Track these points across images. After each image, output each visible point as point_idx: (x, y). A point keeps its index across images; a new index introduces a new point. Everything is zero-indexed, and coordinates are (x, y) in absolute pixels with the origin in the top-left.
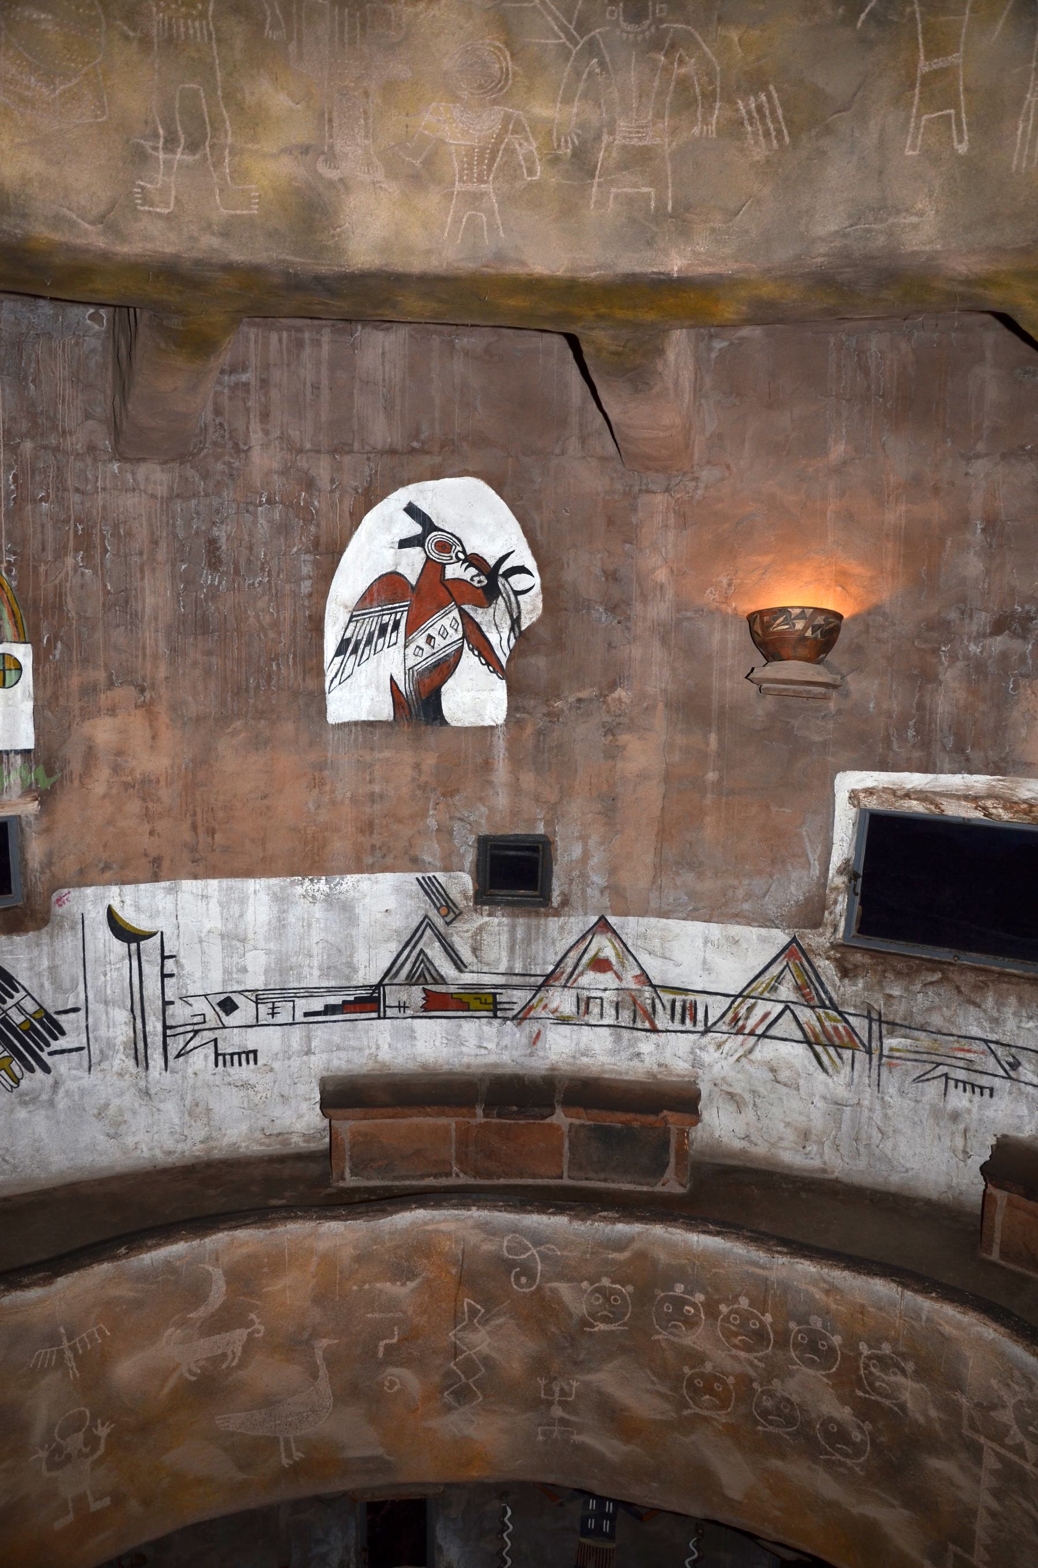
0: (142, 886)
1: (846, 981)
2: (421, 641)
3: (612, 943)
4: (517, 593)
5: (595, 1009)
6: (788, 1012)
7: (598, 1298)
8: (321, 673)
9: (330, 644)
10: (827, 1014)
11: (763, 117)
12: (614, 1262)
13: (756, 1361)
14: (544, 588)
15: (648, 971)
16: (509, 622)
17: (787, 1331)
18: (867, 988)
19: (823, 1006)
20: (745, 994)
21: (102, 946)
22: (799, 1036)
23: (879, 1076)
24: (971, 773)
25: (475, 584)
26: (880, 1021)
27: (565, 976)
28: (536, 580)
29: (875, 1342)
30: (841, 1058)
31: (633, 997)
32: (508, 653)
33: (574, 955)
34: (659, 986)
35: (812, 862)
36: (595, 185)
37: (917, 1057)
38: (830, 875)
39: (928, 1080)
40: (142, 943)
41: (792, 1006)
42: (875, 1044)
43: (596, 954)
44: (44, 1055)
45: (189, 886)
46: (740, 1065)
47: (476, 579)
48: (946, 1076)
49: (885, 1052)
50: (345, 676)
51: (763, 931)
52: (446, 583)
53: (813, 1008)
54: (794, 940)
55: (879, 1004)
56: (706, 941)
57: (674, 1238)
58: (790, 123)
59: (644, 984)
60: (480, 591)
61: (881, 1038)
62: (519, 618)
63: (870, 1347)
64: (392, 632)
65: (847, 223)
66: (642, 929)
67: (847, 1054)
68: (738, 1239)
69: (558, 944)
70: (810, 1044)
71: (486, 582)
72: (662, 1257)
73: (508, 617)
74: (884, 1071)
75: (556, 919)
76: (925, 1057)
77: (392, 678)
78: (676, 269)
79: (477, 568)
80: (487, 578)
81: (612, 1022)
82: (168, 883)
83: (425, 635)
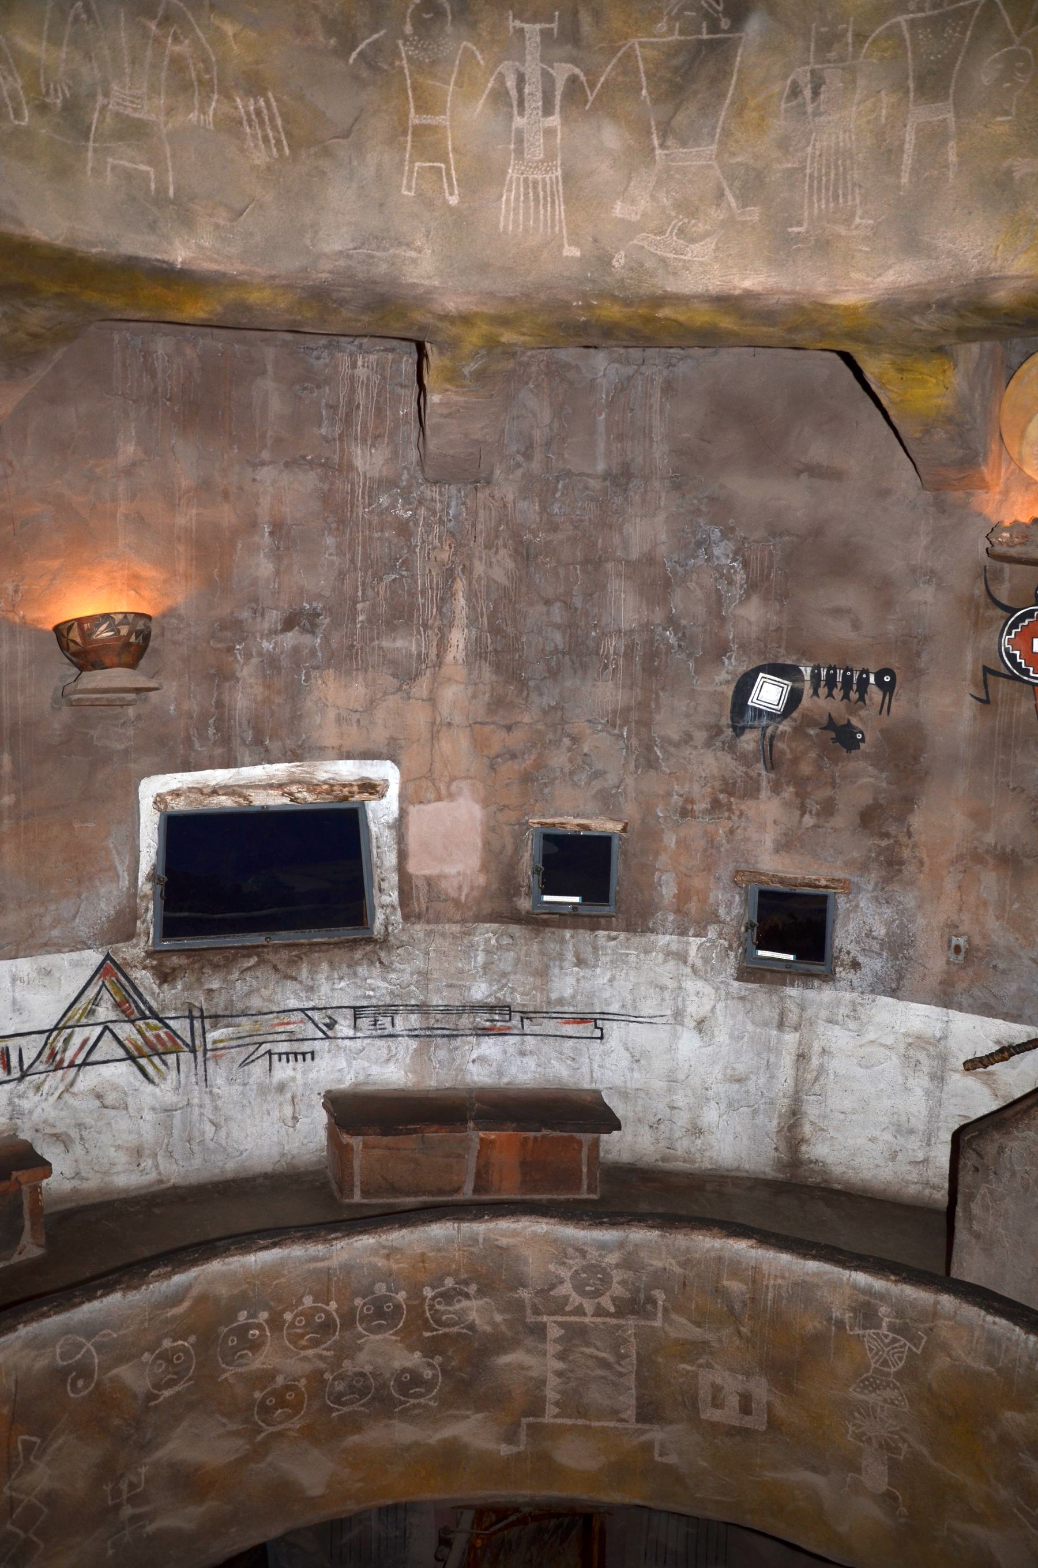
1: (165, 986)
6: (107, 1033)
7: (161, 1365)
10: (147, 1024)
11: (262, 123)
12: (174, 1318)
13: (325, 1353)
17: (353, 1309)
18: (187, 988)
19: (144, 1017)
20: (60, 1025)
22: (121, 1053)
23: (206, 1071)
24: (270, 762)
29: (437, 1282)
30: (165, 1063)
35: (121, 873)
36: (91, 149)
37: (240, 1042)
38: (140, 883)
39: (253, 1061)
41: (111, 1025)
46: (63, 1101)
48: (270, 1053)
49: (209, 1046)
51: (75, 955)
53: (133, 1022)
54: (108, 957)
55: (200, 999)
56: (14, 979)
57: (232, 1267)
58: (289, 135)
61: (204, 1033)
63: (433, 1288)
65: (351, 246)
67: (171, 1059)
68: (293, 1242)
72: (224, 1292)
74: (211, 1065)
76: (247, 1040)
78: (180, 260)
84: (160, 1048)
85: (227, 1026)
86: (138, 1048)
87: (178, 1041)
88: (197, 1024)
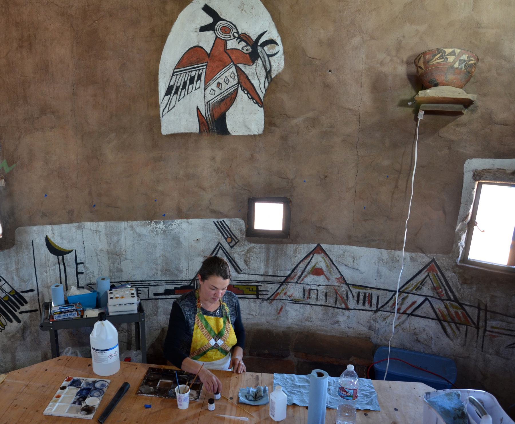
0: (64, 226)
1: (465, 286)
2: (214, 86)
3: (324, 260)
4: (269, 56)
5: (313, 295)
6: (427, 302)
8: (157, 106)
9: (162, 90)
10: (450, 303)
14: (285, 53)
15: (344, 276)
16: (265, 73)
19: (449, 299)
21: (44, 257)
22: (433, 315)
23: (483, 342)
25: (245, 51)
26: (486, 310)
27: (297, 277)
28: (280, 48)
30: (458, 329)
31: (335, 290)
32: (264, 91)
33: (302, 266)
34: (350, 284)
40: (65, 256)
41: (430, 299)
42: (481, 323)
43: (315, 265)
44: (17, 314)
45: (88, 225)
47: (245, 48)
49: (488, 328)
50: (171, 107)
52: (227, 51)
53: (443, 300)
59: (341, 283)
60: (247, 55)
62: (270, 70)
64: (197, 81)
66: (341, 252)
67: (463, 328)
69: (293, 259)
70: (438, 319)
71: (251, 50)
73: (264, 71)
75: (292, 245)
77: (197, 108)
79: (245, 42)
80: (251, 47)
81: (323, 303)
82: (77, 224)
83: (216, 83)
84: (457, 320)
85: (502, 321)
86: (443, 315)
87: (469, 319)
88: (482, 313)
